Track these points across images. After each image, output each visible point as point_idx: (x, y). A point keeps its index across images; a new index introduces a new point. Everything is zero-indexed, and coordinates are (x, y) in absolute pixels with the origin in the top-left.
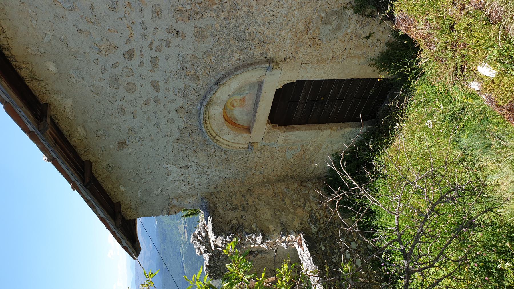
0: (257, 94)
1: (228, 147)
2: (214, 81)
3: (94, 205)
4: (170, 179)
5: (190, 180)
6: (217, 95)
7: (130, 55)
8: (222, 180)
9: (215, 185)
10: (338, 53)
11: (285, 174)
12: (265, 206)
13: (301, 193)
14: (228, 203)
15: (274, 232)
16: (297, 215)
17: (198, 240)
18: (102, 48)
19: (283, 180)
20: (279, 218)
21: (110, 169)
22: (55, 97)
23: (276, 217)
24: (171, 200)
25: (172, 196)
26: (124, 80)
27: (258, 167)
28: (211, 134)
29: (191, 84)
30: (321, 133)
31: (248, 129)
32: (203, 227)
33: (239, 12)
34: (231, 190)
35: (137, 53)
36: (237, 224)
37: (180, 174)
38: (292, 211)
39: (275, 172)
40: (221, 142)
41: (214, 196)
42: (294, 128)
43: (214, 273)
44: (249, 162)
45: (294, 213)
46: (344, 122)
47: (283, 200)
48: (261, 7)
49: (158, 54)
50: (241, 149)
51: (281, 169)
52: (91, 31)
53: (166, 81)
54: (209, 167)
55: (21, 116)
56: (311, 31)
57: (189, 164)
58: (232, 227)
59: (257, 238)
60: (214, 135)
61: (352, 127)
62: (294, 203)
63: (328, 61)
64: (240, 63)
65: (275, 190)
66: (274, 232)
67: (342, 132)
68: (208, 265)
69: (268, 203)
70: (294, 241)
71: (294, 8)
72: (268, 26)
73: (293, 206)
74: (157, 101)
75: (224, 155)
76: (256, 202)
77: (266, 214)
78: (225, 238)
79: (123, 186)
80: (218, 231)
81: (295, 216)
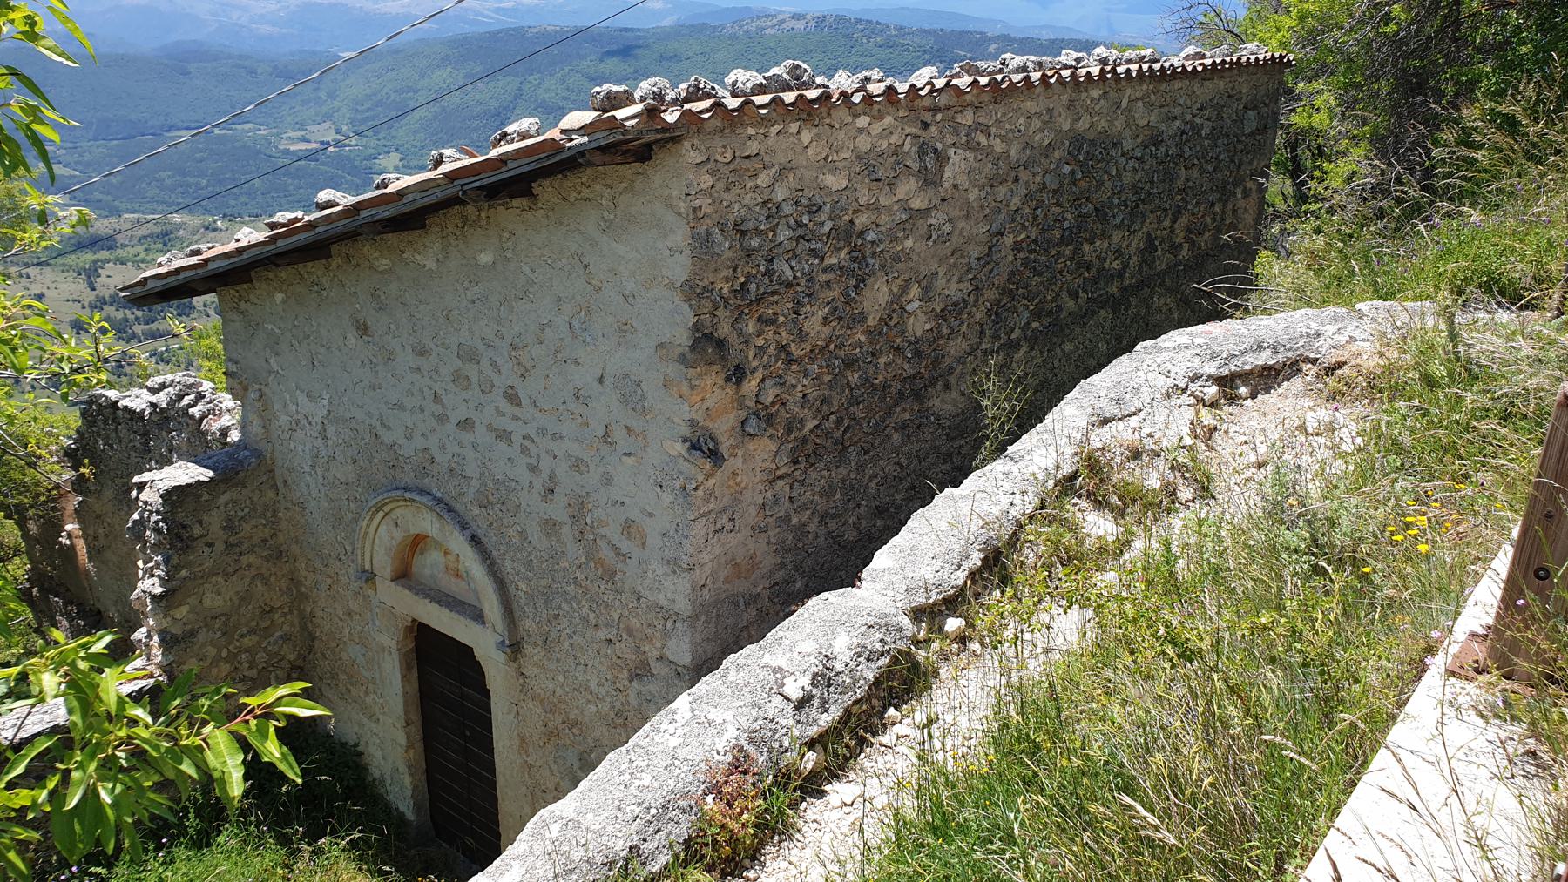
0: (469, 605)
1: (363, 530)
2: (481, 533)
3: (232, 260)
4: (301, 397)
5: (299, 434)
6: (457, 533)
7: (513, 397)
8: (301, 500)
9: (289, 482)
10: (538, 777)
11: (318, 634)
12: (237, 593)
13: (272, 668)
14: (247, 510)
15: (169, 619)
16: (214, 664)
17: (180, 397)
18: (520, 352)
19: (304, 628)
20: (206, 625)
21: (316, 288)
22: (437, 244)
23: (209, 619)
24: (257, 386)
25: (266, 390)
26: (471, 371)
27: (329, 581)
28: (387, 503)
29: (472, 490)
30: (398, 726)
31: (403, 575)
32: (214, 410)
33: (587, 606)
34: (280, 514)
35: (516, 411)
36: (191, 536)
37: (310, 418)
38: (224, 654)
39: (321, 613)
40: (371, 519)
41: (264, 478)
42: (409, 668)
43: (99, 412)
44: (338, 563)
45: (217, 660)
46: (427, 771)
47: (252, 632)
48: (596, 647)
49: (517, 445)
50: (359, 557)
51: (326, 628)
52: (543, 346)
53: (475, 447)
54: (326, 481)
55: (382, 208)
56: (567, 731)
57: (330, 442)
58: (185, 527)
59: (156, 580)
60: (386, 509)
61: (413, 790)
62: (243, 656)
63: (525, 757)
64: (512, 589)
65: (280, 611)
66: (169, 619)
67: (403, 768)
68: (119, 404)
69: (245, 598)
70: (148, 660)
71: (600, 706)
72: (572, 653)
73: (236, 655)
74: (442, 419)
75: (350, 516)
76: (247, 573)
77: (216, 598)
78: (158, 512)
79: (284, 302)
80: (175, 498)
81: (209, 661)
